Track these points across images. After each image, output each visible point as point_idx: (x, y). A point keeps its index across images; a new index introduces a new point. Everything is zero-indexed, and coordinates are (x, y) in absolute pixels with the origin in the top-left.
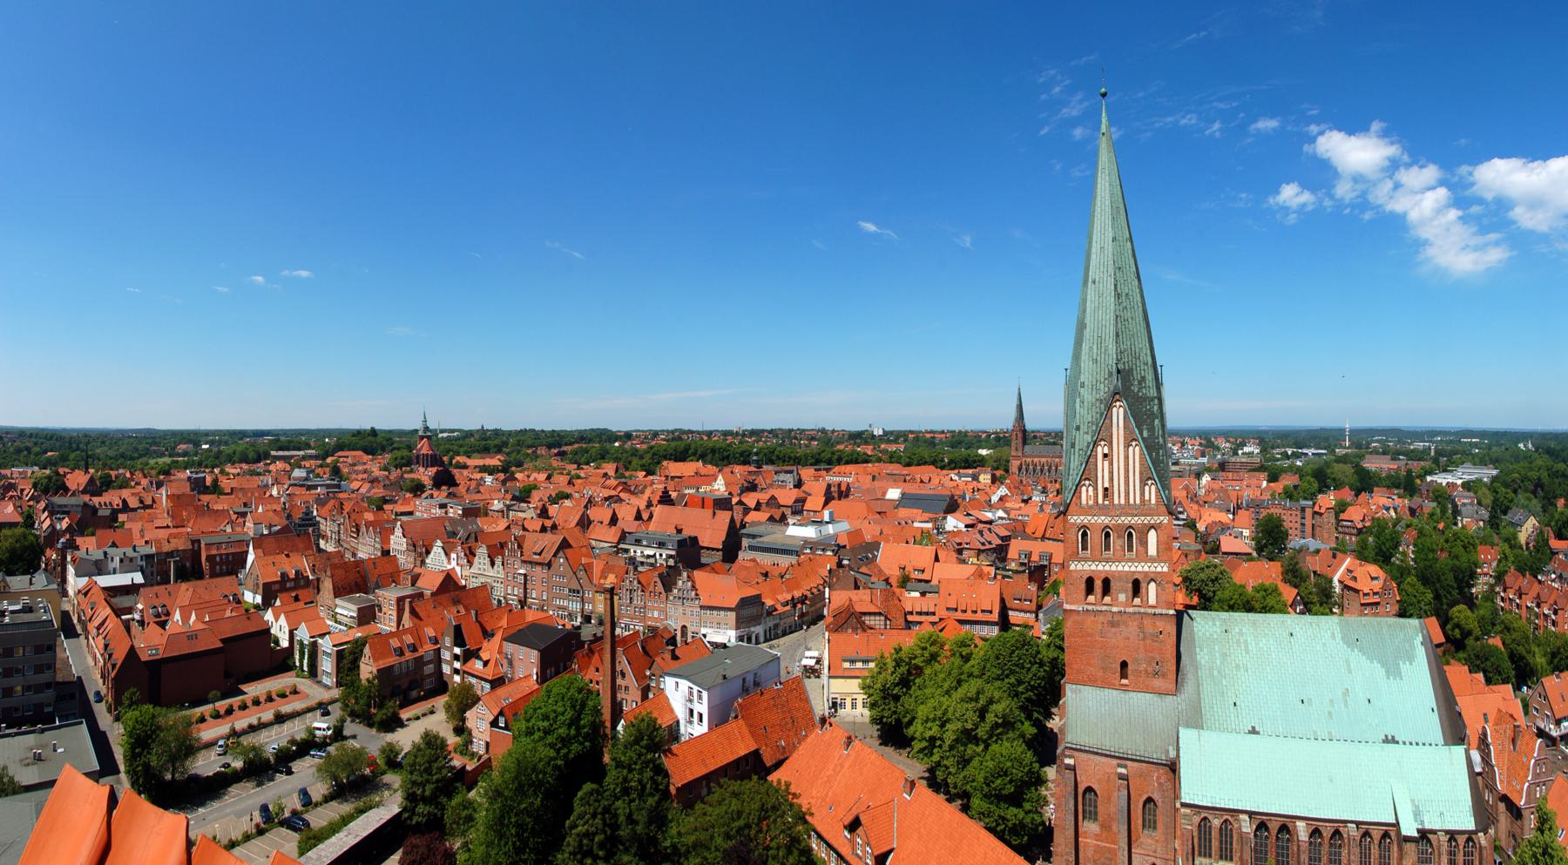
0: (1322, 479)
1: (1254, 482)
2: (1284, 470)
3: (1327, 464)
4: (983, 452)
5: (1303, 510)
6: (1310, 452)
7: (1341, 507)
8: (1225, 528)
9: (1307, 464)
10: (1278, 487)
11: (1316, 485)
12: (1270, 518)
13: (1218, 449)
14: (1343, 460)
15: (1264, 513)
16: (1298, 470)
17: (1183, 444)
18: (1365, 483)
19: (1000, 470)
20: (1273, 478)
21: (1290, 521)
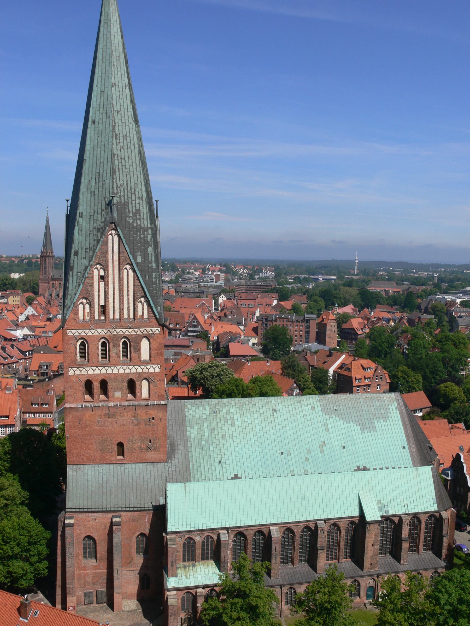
0: (329, 297)
1: (265, 300)
2: (293, 291)
3: (336, 287)
4: (15, 276)
5: (308, 321)
6: (321, 278)
7: (342, 320)
8: (235, 337)
9: (317, 286)
10: (288, 305)
11: (323, 303)
12: (275, 329)
13: (234, 273)
14: (350, 284)
15: (270, 325)
16: (306, 292)
17: (204, 270)
18: (367, 301)
19: (31, 289)
20: (283, 297)
21: (295, 330)
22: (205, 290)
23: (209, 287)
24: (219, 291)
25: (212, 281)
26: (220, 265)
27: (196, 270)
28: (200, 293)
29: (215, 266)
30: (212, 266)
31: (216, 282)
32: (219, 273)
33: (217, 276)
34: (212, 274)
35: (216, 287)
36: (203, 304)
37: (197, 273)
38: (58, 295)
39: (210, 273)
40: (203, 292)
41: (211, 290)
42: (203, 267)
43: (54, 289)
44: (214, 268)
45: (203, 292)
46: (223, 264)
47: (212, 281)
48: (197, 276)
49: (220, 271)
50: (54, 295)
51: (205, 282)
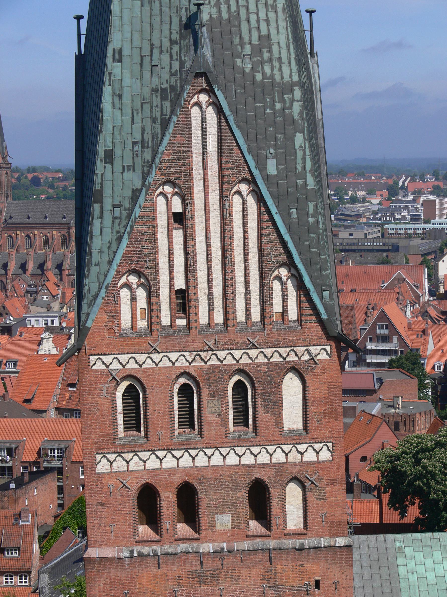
17: (393, 190)
22: (402, 243)
23: (410, 236)
24: (437, 244)
25: (415, 218)
26: (435, 174)
27: (371, 193)
28: (388, 252)
29: (422, 178)
30: (413, 180)
31: (426, 222)
32: (433, 197)
33: (430, 206)
34: (415, 201)
35: (426, 234)
36: (401, 280)
37: (375, 200)
38: (23, 267)
39: (410, 197)
40: (396, 249)
41: (417, 241)
42: (390, 182)
43: (13, 252)
44: (419, 184)
45: (396, 249)
46: (442, 173)
47: (415, 218)
48: (376, 208)
49: (436, 191)
50: (13, 267)
51: (397, 221)
